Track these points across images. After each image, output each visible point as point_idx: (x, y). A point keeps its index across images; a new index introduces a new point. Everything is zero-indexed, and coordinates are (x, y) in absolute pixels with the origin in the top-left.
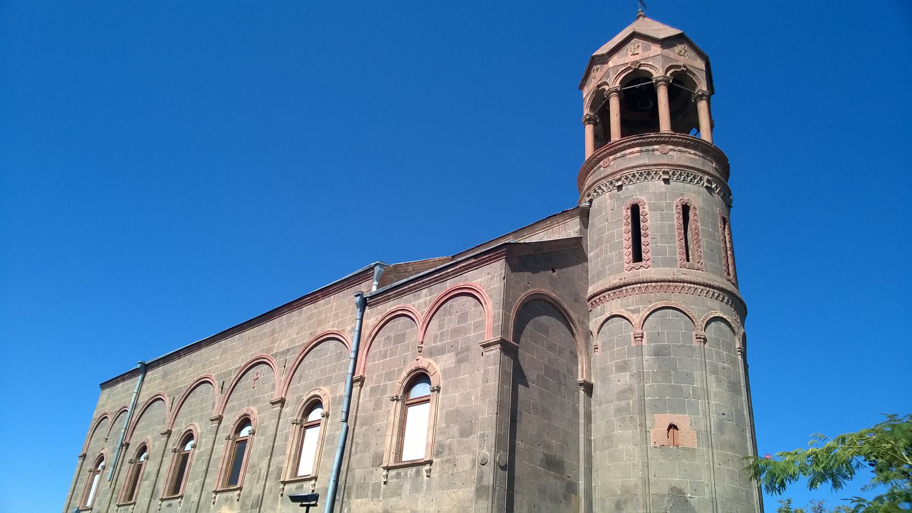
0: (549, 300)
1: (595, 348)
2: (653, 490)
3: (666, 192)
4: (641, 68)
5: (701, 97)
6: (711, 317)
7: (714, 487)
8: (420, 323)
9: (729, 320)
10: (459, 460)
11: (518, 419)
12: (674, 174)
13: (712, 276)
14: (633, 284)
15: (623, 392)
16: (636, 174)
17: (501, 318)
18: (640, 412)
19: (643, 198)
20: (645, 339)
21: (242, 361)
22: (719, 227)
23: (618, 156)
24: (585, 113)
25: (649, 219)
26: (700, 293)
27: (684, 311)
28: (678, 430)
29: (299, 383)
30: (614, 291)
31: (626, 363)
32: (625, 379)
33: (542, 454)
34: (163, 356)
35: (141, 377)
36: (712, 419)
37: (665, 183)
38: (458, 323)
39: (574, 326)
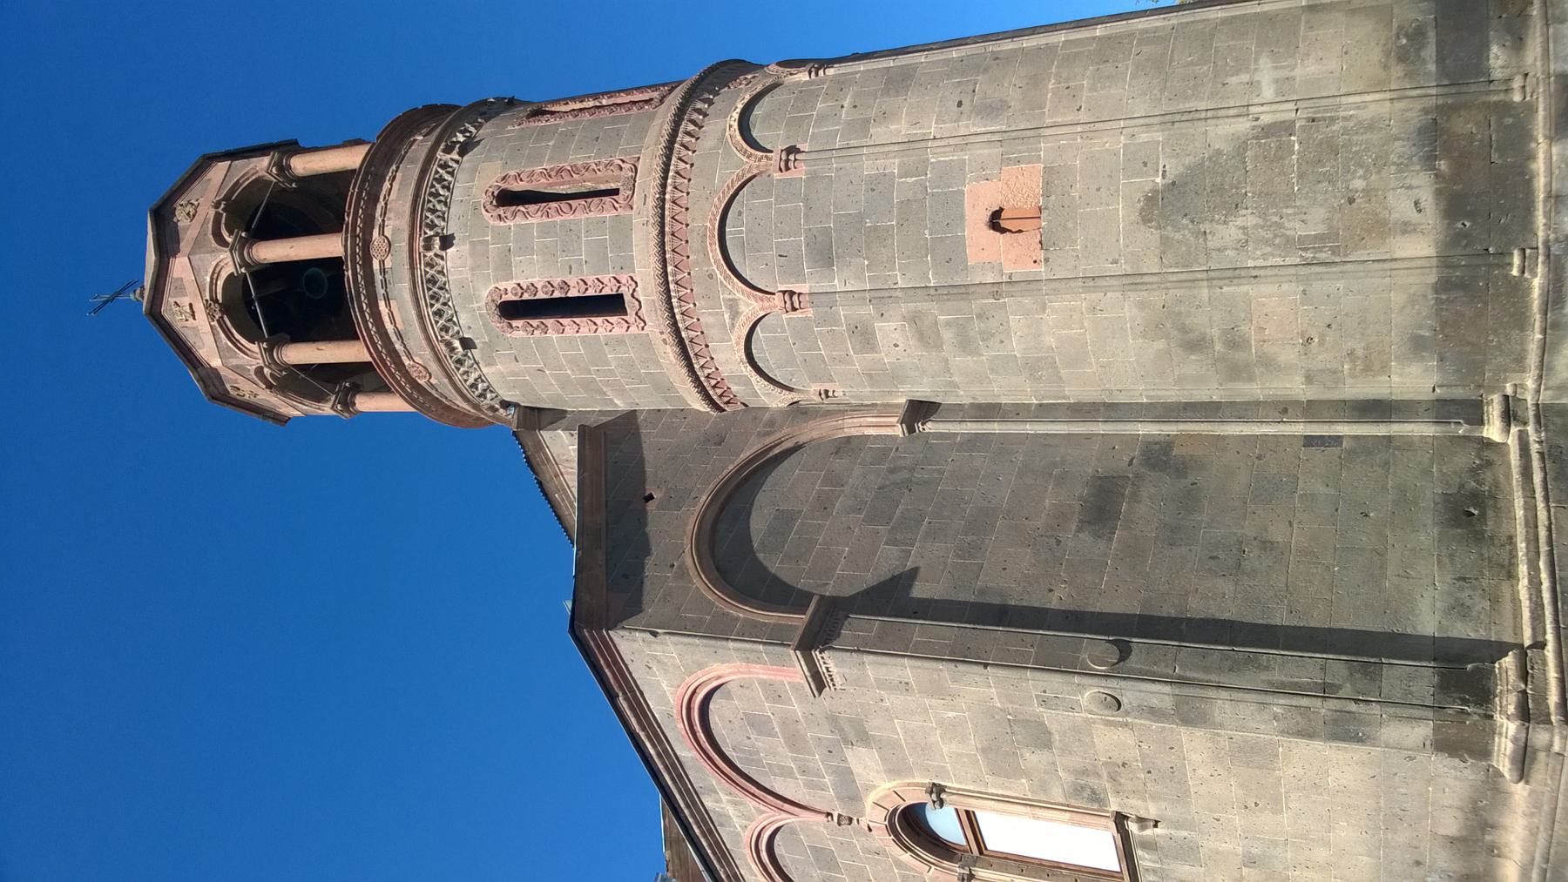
0: (716, 507)
1: (827, 397)
2: (1151, 265)
3: (470, 242)
4: (220, 297)
5: (283, 169)
6: (739, 138)
7: (1136, 121)
8: (782, 819)
9: (748, 97)
10: (1110, 754)
11: (996, 601)
12: (432, 226)
13: (650, 137)
14: (673, 316)
15: (921, 336)
16: (434, 309)
17: (748, 646)
18: (964, 296)
19: (484, 292)
20: (796, 288)
23: (402, 348)
25: (530, 280)
26: (686, 163)
27: (727, 199)
28: (1001, 210)
30: (692, 355)
32: (890, 330)
36: (973, 130)
37: (452, 245)
38: (775, 735)
39: (777, 445)
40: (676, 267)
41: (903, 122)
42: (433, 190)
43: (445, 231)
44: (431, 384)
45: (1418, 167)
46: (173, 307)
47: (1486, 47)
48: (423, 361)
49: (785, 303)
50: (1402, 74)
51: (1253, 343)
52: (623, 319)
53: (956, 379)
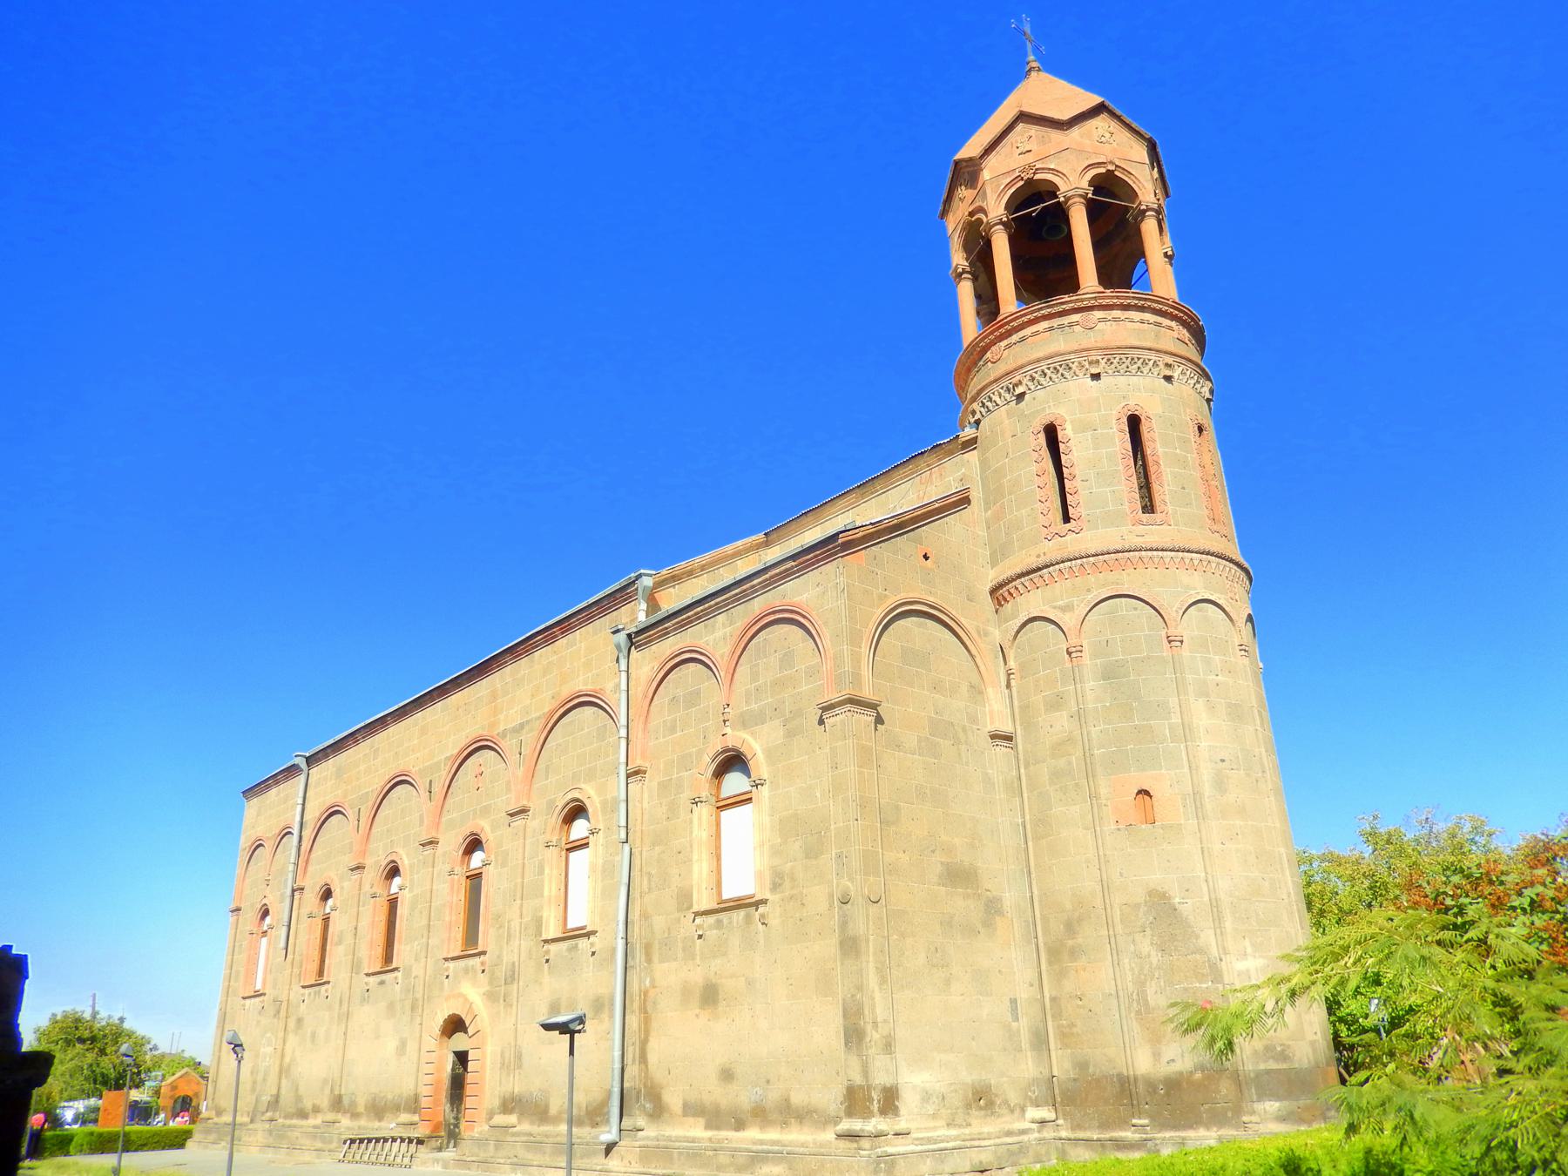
4: (1038, 177)
14: (1058, 563)
16: (1046, 371)
20: (1086, 654)
21: (455, 744)
23: (1013, 341)
24: (954, 264)
25: (1074, 448)
28: (1151, 797)
29: (547, 779)
30: (1030, 577)
31: (1060, 696)
33: (939, 865)
34: (331, 741)
35: (302, 778)
42: (1136, 360)
45: (1196, 1061)
47: (1278, 1099)
50: (1257, 1048)
51: (1075, 964)
53: (1032, 768)
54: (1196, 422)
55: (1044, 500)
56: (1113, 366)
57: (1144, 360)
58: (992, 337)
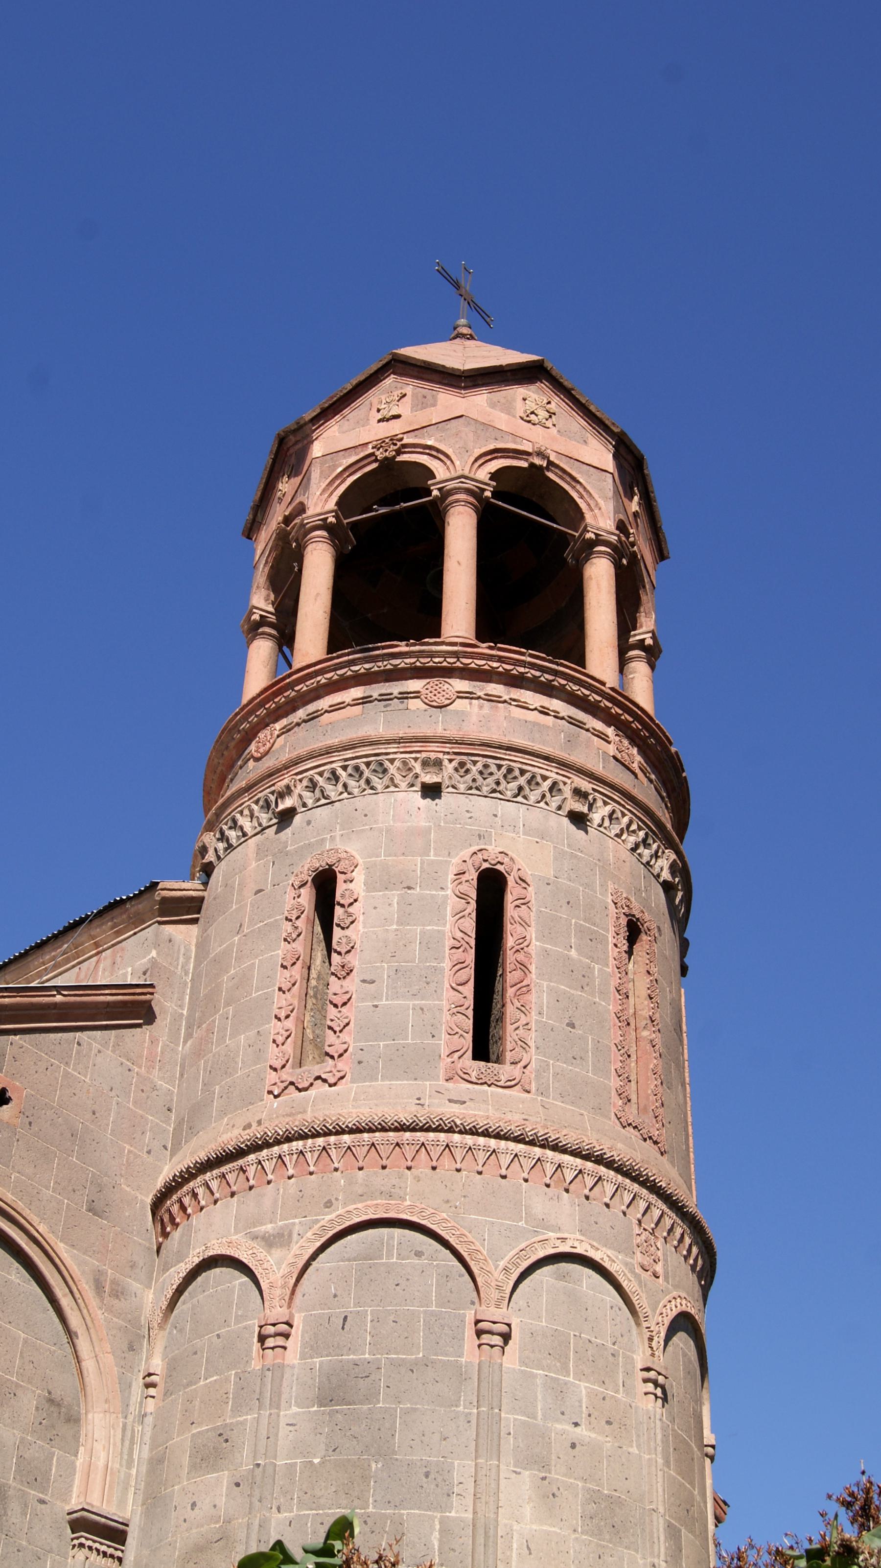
3: (428, 830)
14: (278, 1142)
16: (340, 771)
22: (611, 946)
23: (295, 721)
25: (361, 918)
30: (223, 1169)
40: (349, 1148)
41: (534, 1527)
42: (517, 773)
43: (451, 790)
44: (249, 759)
46: (400, 391)
48: (277, 750)
49: (274, 1325)
52: (287, 1061)
54: (626, 910)
55: (282, 1015)
56: (469, 777)
57: (533, 777)
58: (262, 712)
